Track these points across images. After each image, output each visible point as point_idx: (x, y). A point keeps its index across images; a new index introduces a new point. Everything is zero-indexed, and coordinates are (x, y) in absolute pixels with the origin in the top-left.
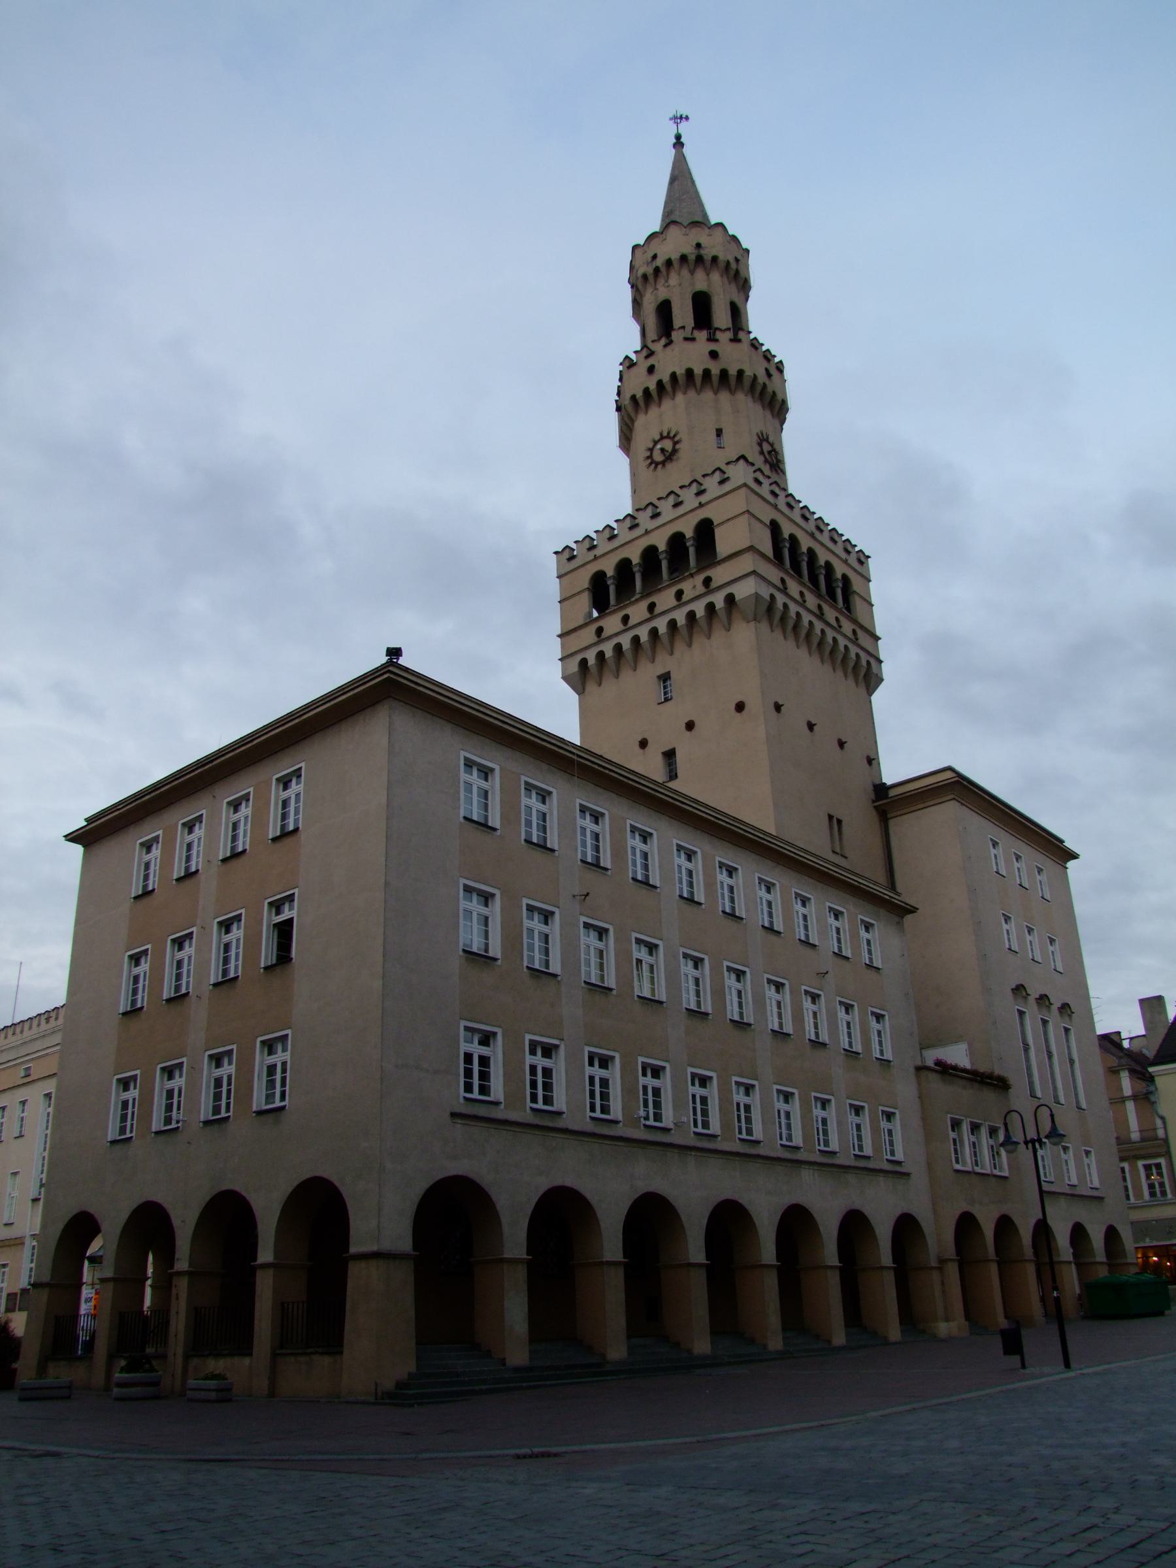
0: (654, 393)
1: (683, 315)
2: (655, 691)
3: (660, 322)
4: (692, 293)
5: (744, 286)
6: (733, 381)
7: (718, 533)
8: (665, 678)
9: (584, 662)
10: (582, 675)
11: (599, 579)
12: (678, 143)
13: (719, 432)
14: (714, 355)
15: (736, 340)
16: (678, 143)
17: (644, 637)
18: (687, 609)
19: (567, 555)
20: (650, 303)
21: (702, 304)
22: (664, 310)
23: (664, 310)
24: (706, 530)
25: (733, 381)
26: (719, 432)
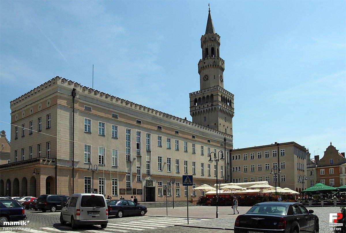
0: (205, 67)
1: (210, 51)
2: (203, 119)
3: (206, 53)
4: (210, 44)
5: (219, 44)
6: (217, 66)
7: (214, 96)
8: (205, 117)
9: (193, 113)
10: (193, 114)
11: (196, 99)
12: (209, 11)
13: (214, 76)
14: (214, 62)
15: (218, 59)
16: (209, 11)
17: (202, 111)
18: (209, 108)
19: (191, 94)
20: (204, 47)
21: (213, 49)
22: (207, 49)
23: (207, 49)
24: (212, 95)
25: (217, 66)
26: (214, 76)
